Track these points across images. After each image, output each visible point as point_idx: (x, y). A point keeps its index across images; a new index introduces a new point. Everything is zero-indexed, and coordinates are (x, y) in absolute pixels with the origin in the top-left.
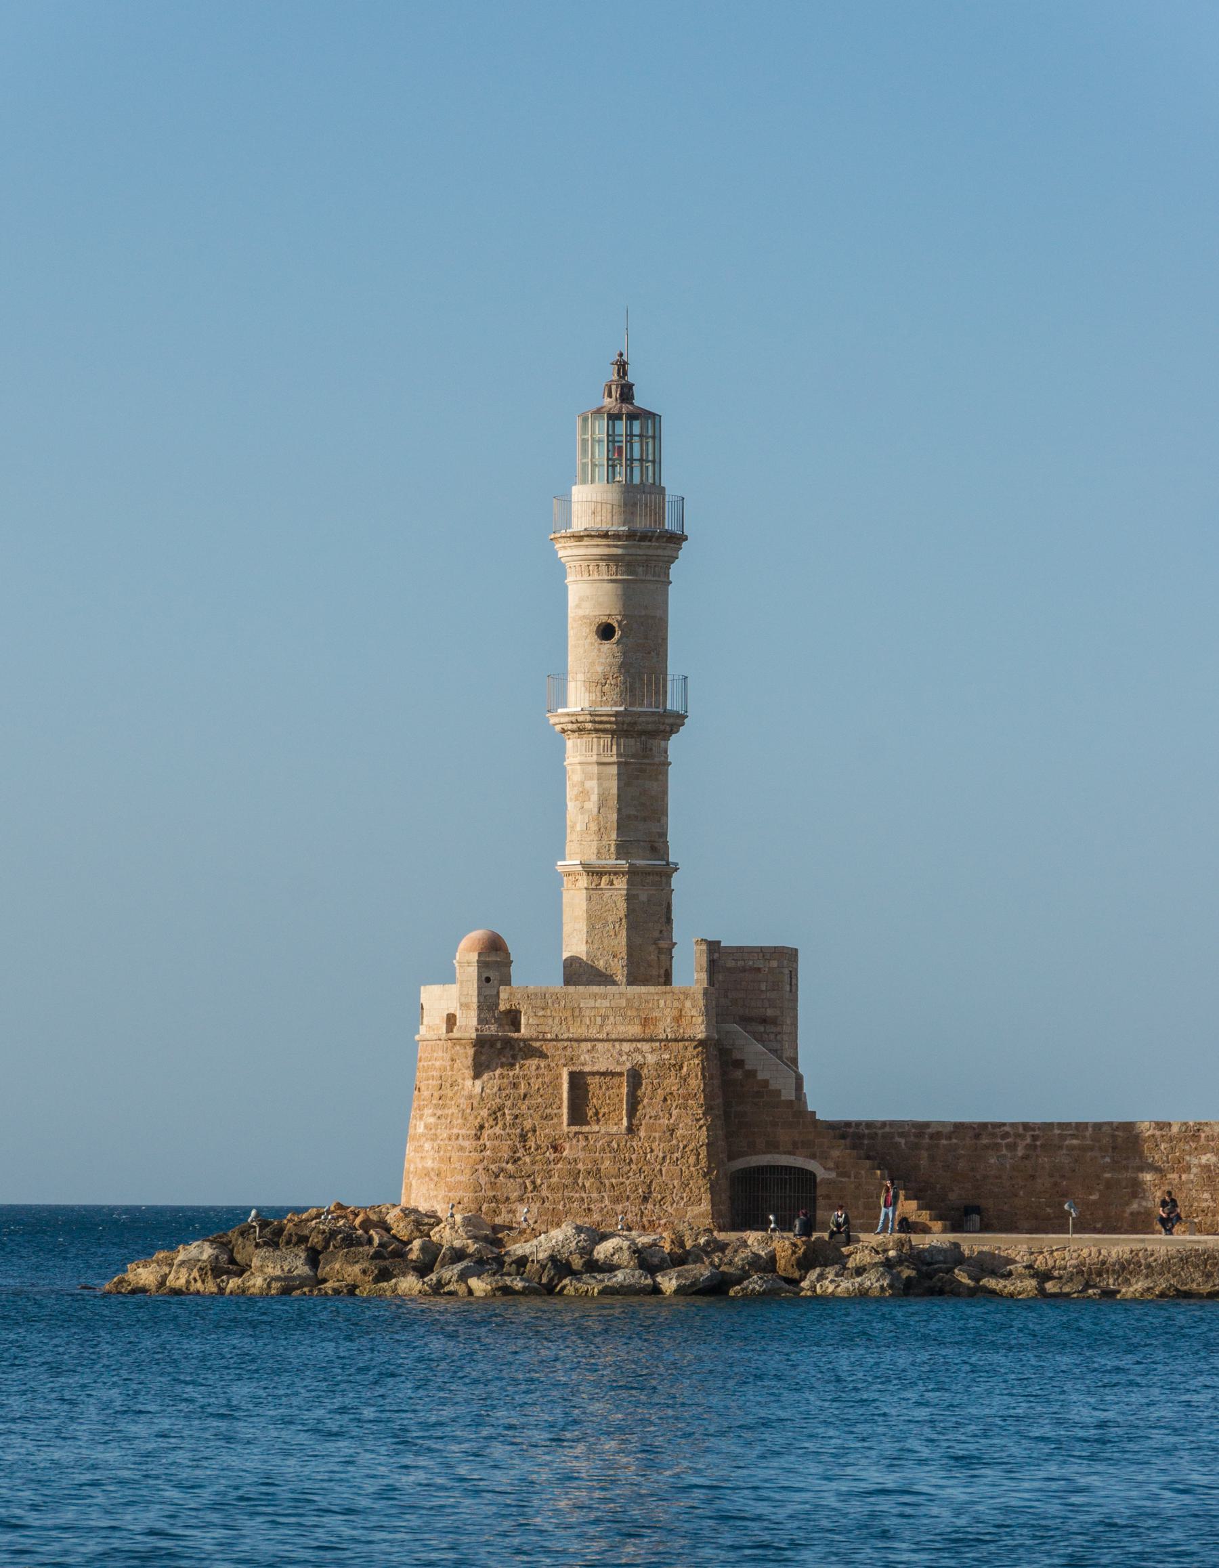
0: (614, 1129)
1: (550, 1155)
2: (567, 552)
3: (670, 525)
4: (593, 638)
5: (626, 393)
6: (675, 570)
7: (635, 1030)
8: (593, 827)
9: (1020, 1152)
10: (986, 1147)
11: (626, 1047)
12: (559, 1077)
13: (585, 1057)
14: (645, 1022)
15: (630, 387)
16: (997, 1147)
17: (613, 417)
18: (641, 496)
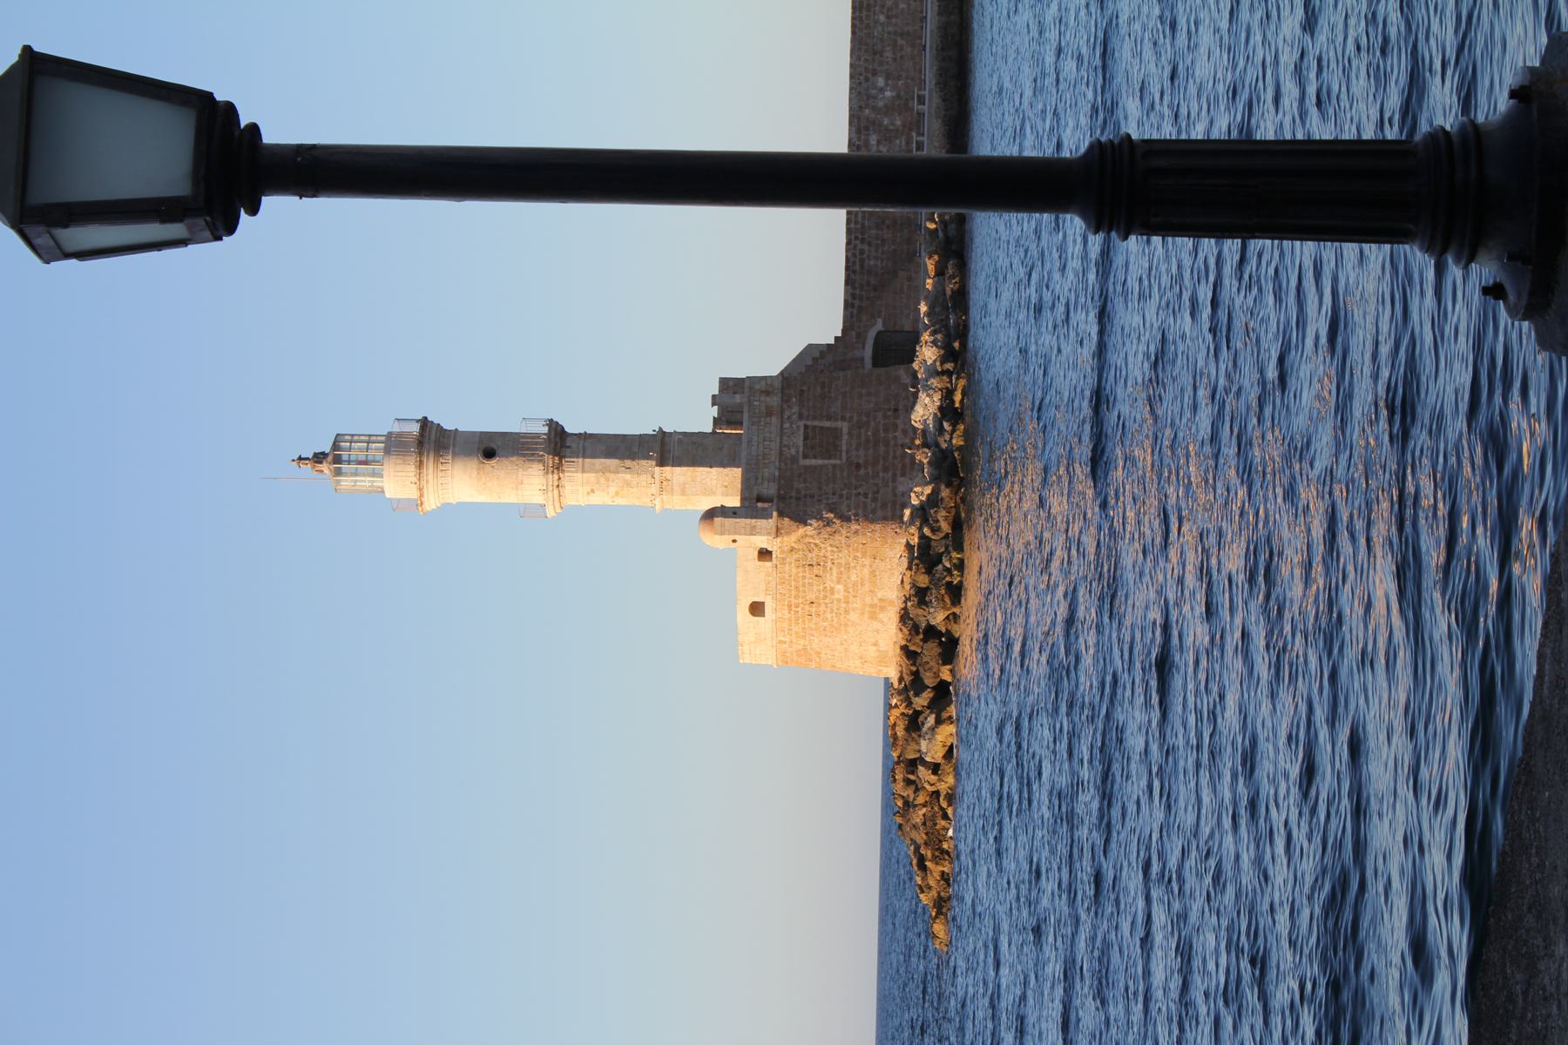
0: (845, 430)
1: (862, 472)
2: (431, 503)
3: (415, 428)
4: (493, 462)
5: (319, 458)
6: (448, 425)
7: (774, 420)
8: (628, 463)
9: (866, 247)
10: (862, 266)
11: (787, 425)
12: (806, 467)
13: (793, 451)
14: (769, 413)
15: (316, 455)
16: (862, 261)
17: (338, 472)
18: (394, 444)
